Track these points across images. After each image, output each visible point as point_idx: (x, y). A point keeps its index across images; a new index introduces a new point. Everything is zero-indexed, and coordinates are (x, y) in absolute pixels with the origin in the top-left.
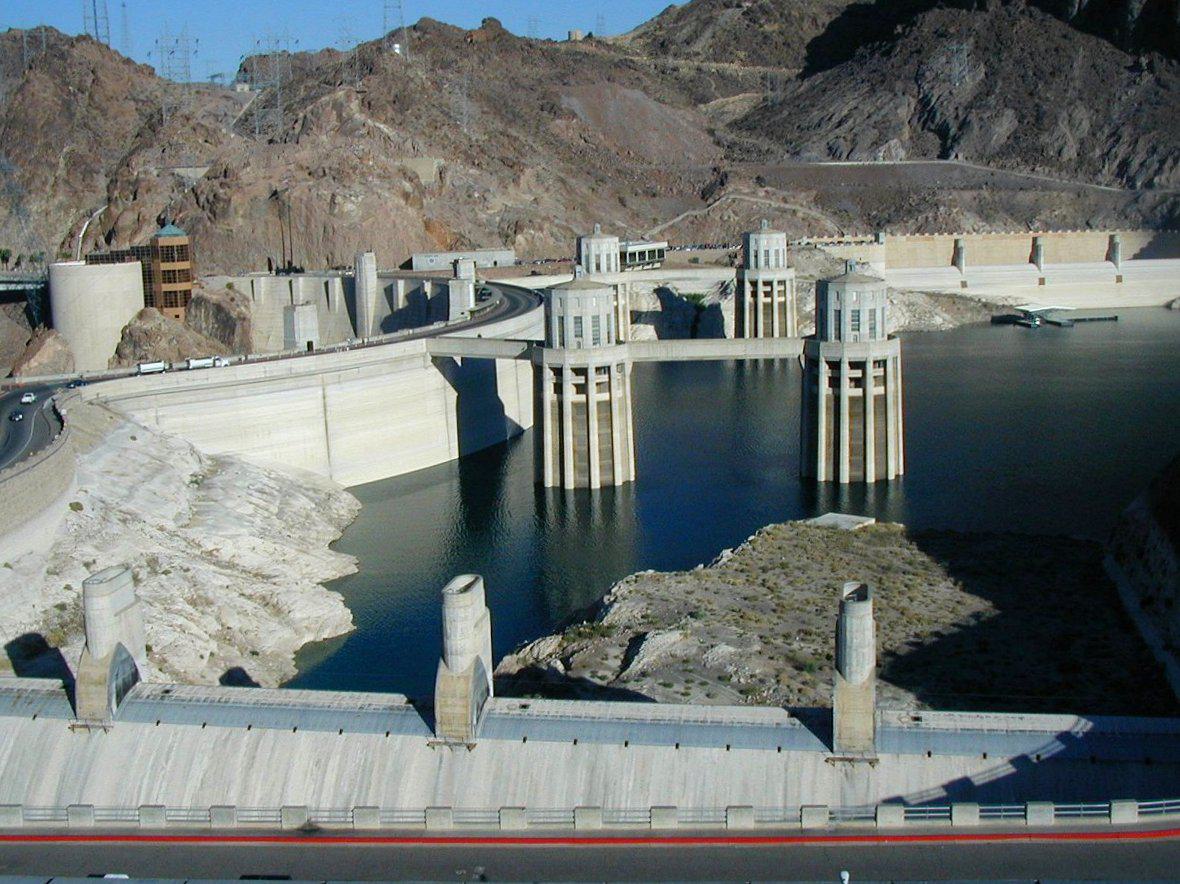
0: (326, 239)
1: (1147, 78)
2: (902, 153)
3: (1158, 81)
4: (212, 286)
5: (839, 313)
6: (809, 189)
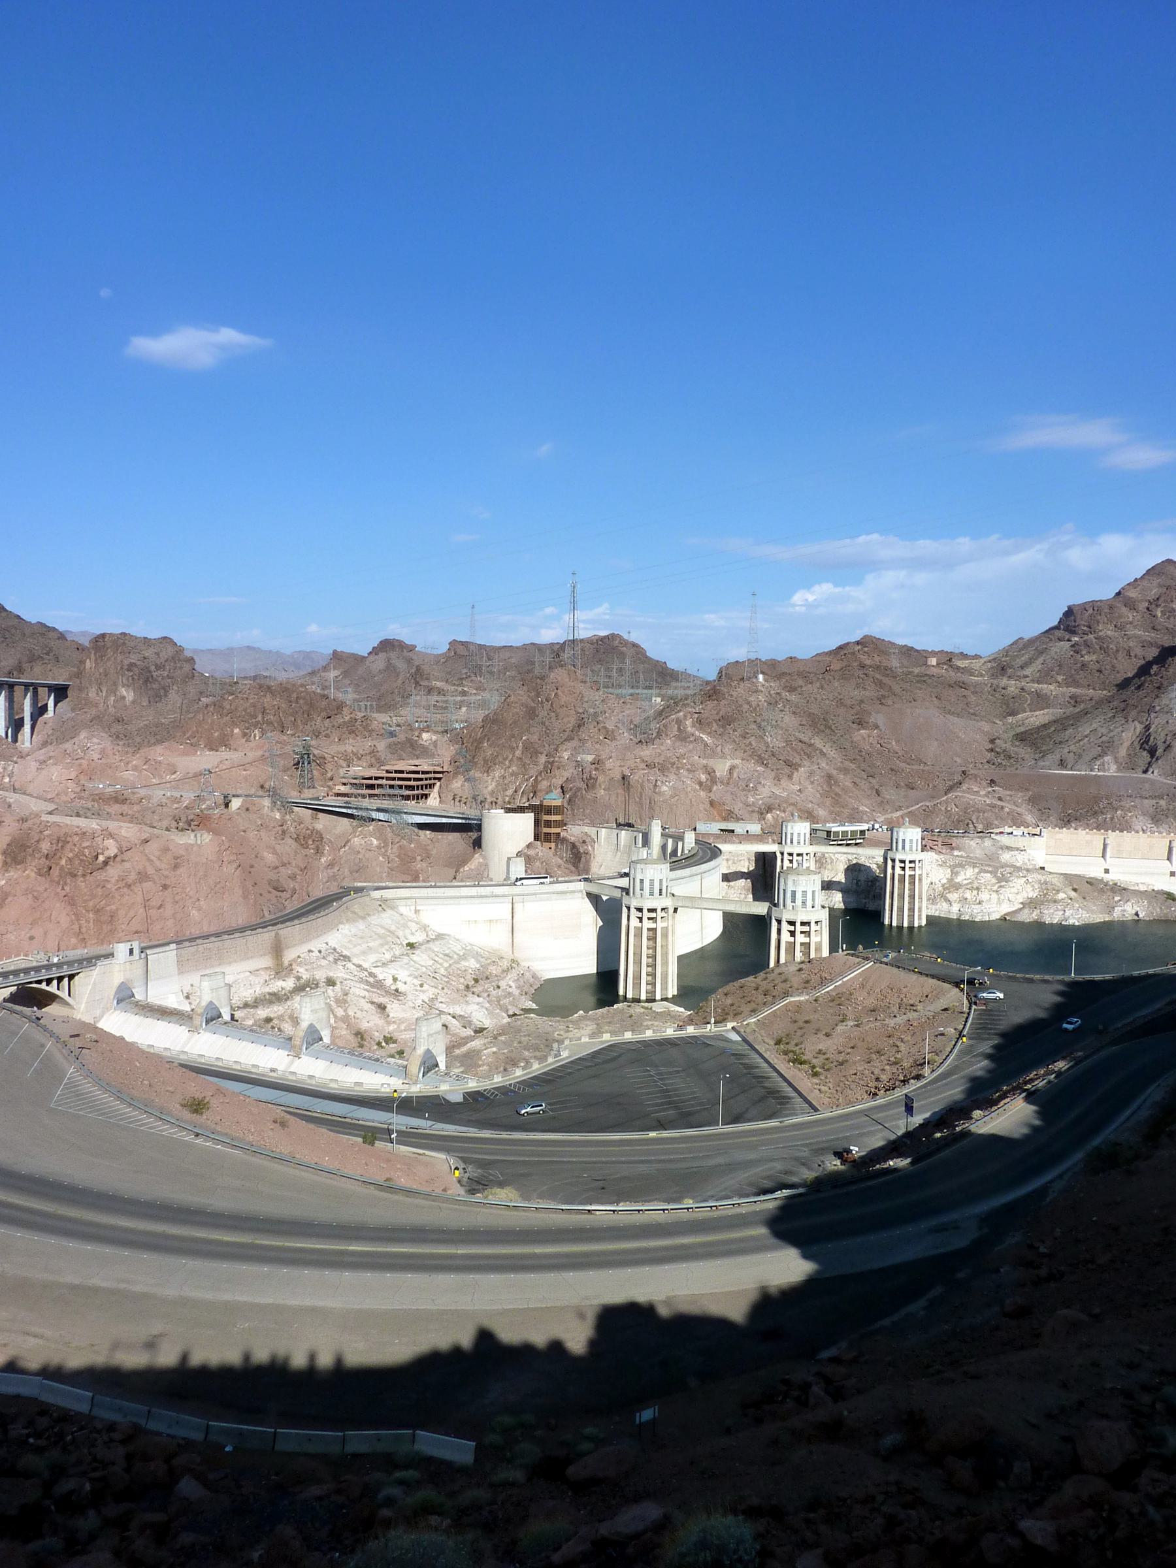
0: (651, 808)
2: (1113, 767)
4: (573, 832)
6: (1028, 790)
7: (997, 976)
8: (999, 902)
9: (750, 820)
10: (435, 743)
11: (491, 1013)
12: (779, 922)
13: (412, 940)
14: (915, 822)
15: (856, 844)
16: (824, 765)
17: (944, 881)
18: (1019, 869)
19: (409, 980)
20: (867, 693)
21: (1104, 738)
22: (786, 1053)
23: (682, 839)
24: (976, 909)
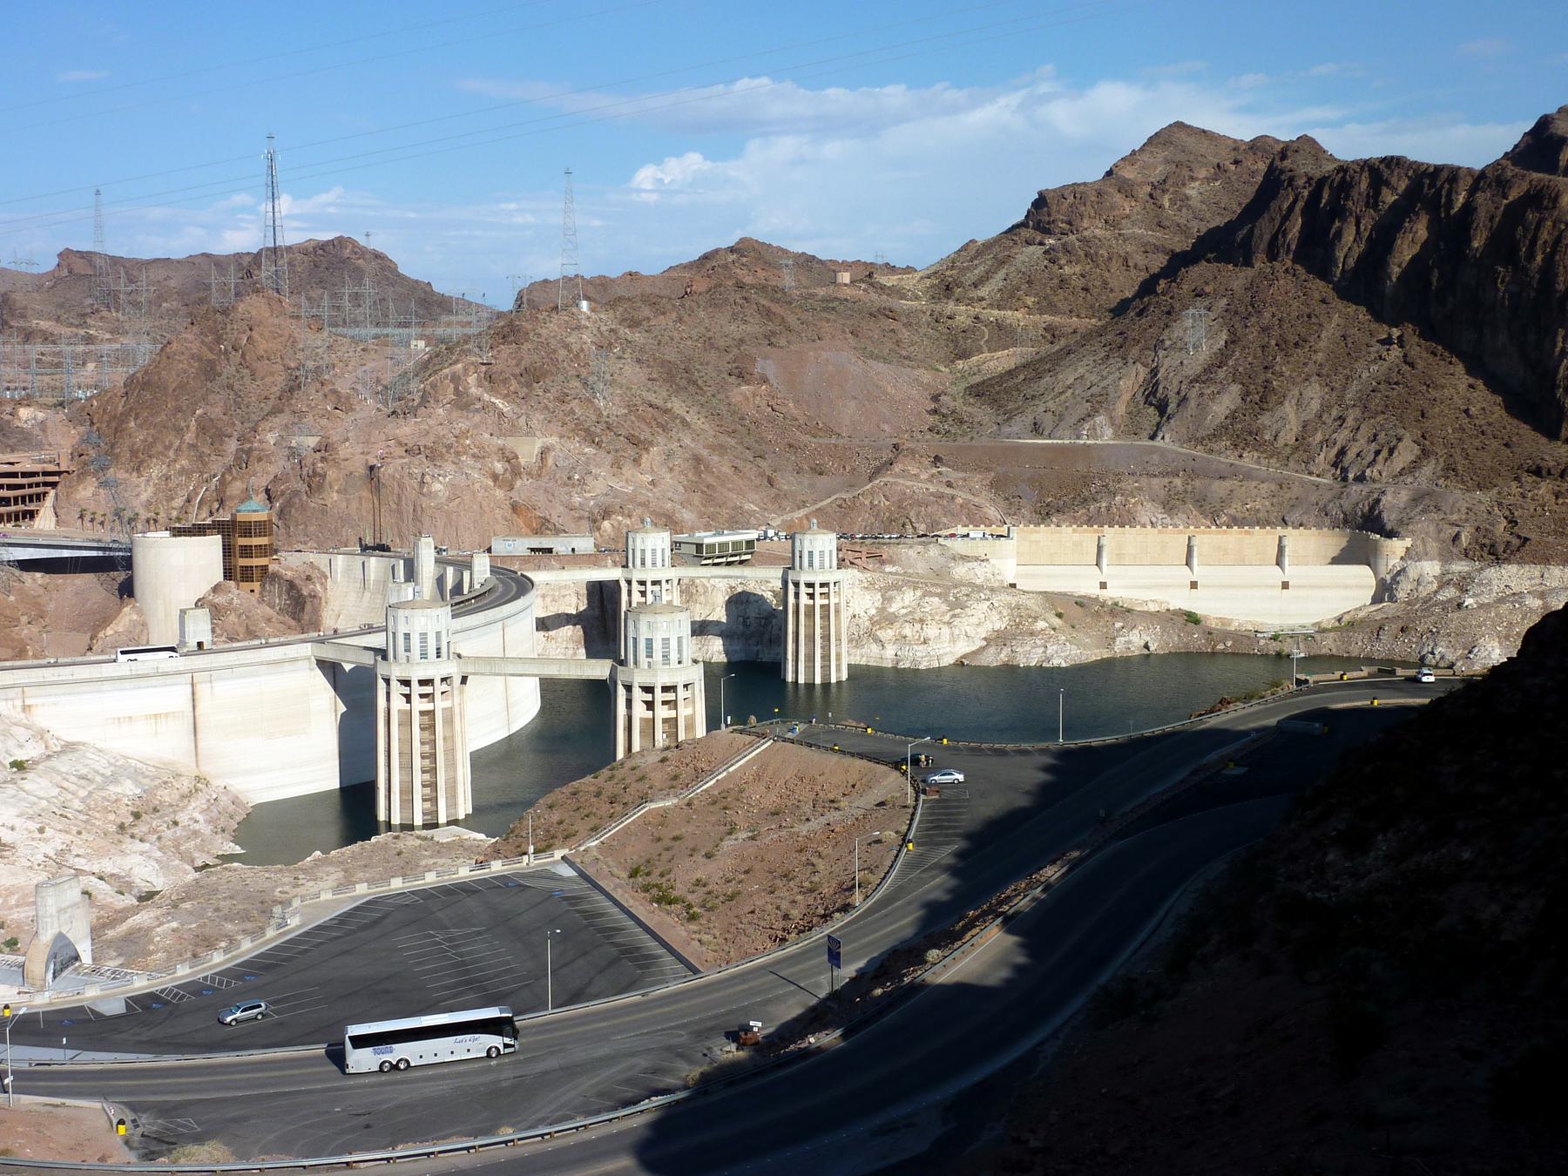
0: (416, 519)
1: (1396, 352)
2: (1109, 432)
4: (290, 563)
6: (988, 470)
7: (955, 749)
8: (953, 639)
9: (577, 533)
10: (43, 425)
11: (164, 867)
12: (629, 688)
13: (21, 756)
14: (826, 525)
15: (741, 562)
16: (687, 441)
17: (873, 612)
18: (980, 588)
19: (18, 822)
20: (749, 328)
21: (1094, 390)
22: (646, 889)
23: (469, 566)
24: (920, 651)
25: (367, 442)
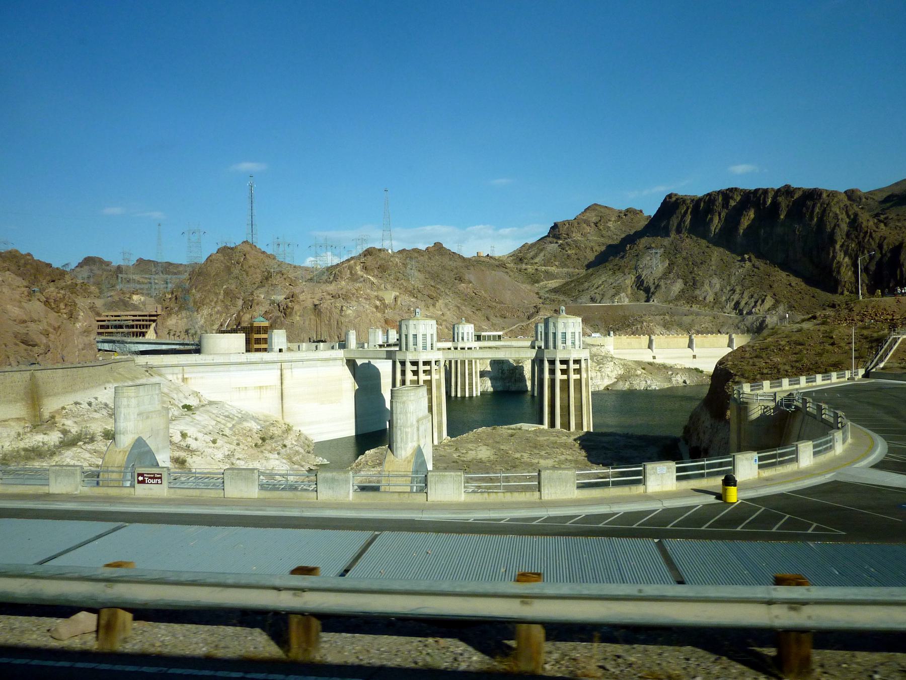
0: (338, 327)
1: (748, 264)
2: (627, 300)
3: (754, 266)
5: (554, 334)
8: (602, 378)
10: (144, 304)
19: (200, 436)
25: (313, 293)
